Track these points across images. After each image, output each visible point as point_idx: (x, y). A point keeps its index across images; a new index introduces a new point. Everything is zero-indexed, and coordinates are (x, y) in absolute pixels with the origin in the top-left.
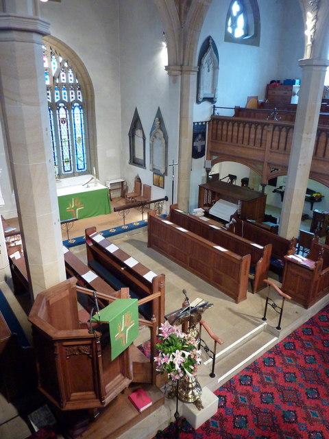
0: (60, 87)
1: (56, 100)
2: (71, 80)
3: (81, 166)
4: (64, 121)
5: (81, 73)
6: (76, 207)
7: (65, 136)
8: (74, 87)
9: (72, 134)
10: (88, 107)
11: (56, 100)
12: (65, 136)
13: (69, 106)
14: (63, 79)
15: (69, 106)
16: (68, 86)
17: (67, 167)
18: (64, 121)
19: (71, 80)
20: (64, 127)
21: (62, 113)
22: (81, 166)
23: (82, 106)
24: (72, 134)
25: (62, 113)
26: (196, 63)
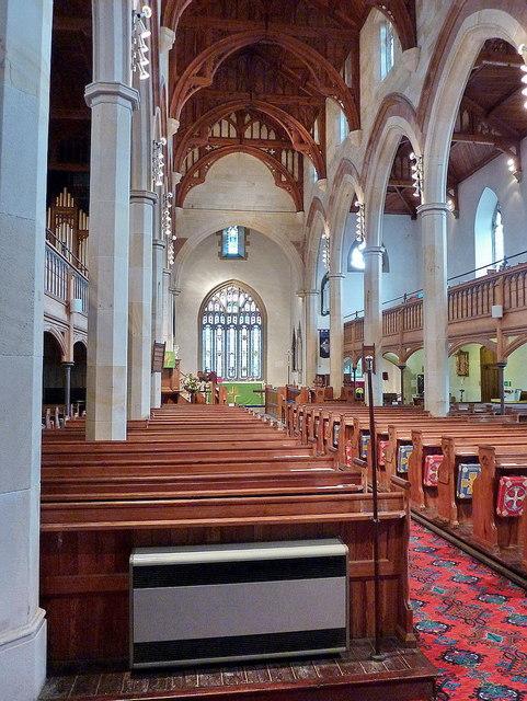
0: (245, 314)
2: (253, 308)
5: (260, 304)
8: (256, 314)
9: (250, 348)
10: (263, 328)
13: (250, 328)
15: (250, 328)
16: (250, 314)
17: (244, 374)
19: (253, 308)
20: (244, 342)
21: (244, 332)
23: (260, 327)
24: (250, 348)
25: (244, 332)
26: (319, 288)
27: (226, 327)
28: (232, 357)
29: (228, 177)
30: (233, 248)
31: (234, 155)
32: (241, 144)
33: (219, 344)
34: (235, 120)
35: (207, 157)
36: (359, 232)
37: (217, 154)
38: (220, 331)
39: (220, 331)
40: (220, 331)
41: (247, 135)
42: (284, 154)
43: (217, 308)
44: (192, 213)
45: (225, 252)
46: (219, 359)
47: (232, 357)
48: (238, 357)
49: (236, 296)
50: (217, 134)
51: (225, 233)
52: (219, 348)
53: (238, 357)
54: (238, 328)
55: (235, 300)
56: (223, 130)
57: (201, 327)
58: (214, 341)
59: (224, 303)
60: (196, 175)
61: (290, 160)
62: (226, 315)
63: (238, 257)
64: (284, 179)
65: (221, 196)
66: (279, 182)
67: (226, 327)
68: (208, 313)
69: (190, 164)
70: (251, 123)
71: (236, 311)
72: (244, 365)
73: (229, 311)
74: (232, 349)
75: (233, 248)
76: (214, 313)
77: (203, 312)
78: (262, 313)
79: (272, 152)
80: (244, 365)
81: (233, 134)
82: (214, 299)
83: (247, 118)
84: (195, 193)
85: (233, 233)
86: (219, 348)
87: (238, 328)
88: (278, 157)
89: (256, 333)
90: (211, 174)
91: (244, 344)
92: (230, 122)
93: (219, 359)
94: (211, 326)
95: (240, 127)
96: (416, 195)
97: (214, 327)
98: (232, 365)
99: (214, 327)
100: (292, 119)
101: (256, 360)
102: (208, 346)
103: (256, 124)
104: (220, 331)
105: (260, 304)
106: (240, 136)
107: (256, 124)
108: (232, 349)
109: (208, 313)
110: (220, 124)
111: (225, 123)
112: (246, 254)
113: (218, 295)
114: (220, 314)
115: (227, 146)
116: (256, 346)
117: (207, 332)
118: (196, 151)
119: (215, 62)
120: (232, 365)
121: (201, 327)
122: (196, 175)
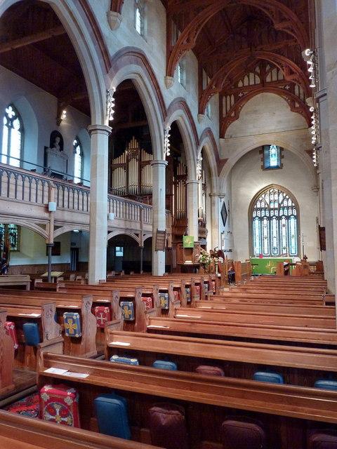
0: (284, 208)
1: (281, 215)
3: (293, 251)
4: (284, 226)
5: (294, 200)
6: (271, 267)
7: (284, 233)
8: (292, 207)
10: (297, 217)
11: (281, 215)
12: (284, 233)
13: (288, 218)
14: (285, 203)
15: (288, 218)
16: (288, 208)
18: (284, 226)
19: (290, 204)
20: (284, 229)
21: (283, 221)
22: (293, 251)
25: (283, 221)
27: (270, 218)
28: (275, 239)
29: (255, 112)
30: (274, 162)
31: (259, 96)
32: (264, 87)
33: (266, 231)
34: (259, 71)
35: (240, 101)
36: (313, 133)
37: (246, 98)
38: (265, 221)
39: (265, 222)
40: (265, 221)
41: (268, 79)
42: (296, 88)
43: (263, 205)
44: (231, 141)
45: (267, 165)
46: (266, 241)
47: (275, 239)
48: (280, 240)
49: (276, 195)
50: (246, 83)
51: (266, 152)
52: (266, 234)
53: (280, 240)
54: (279, 218)
55: (276, 198)
56: (252, 80)
57: (251, 220)
58: (261, 228)
59: (268, 202)
60: (233, 115)
61: (302, 91)
62: (270, 210)
63: (277, 167)
64: (297, 105)
65: (251, 126)
66: (293, 109)
67: (270, 218)
68: (257, 209)
69: (228, 107)
70: (270, 70)
71: (277, 206)
72: (284, 245)
73: (272, 207)
74: (275, 234)
75: (274, 162)
76: (261, 209)
77: (252, 207)
78: (296, 207)
79: (287, 87)
80: (284, 245)
81: (258, 80)
82: (260, 199)
83: (268, 68)
84: (232, 128)
85: (273, 151)
86: (266, 234)
87: (279, 218)
88: (292, 90)
89: (293, 222)
90: (243, 111)
91: (284, 230)
92: (255, 73)
93: (266, 241)
94: (259, 218)
95: (262, 75)
96: (312, 86)
97: (261, 219)
98: (275, 245)
99: (261, 219)
100: (282, 57)
101: (293, 242)
102: (257, 232)
103: (274, 71)
104: (265, 222)
105: (294, 200)
106: (263, 82)
107: (274, 71)
108: (275, 234)
109: (257, 209)
110: (248, 77)
111: (252, 75)
112: (282, 165)
113: (263, 196)
114: (265, 209)
115: (254, 90)
116: (293, 231)
117: (257, 222)
118: (233, 97)
119: (197, 30)
120: (275, 245)
121: (251, 220)
122: (233, 115)
